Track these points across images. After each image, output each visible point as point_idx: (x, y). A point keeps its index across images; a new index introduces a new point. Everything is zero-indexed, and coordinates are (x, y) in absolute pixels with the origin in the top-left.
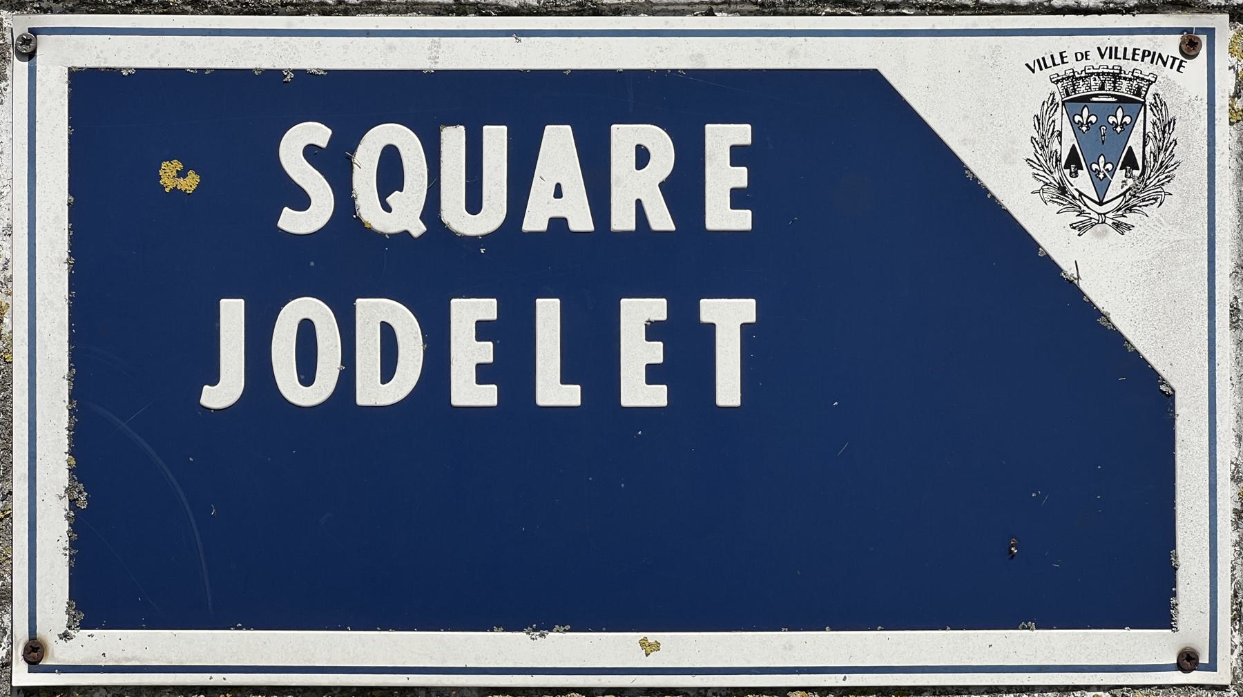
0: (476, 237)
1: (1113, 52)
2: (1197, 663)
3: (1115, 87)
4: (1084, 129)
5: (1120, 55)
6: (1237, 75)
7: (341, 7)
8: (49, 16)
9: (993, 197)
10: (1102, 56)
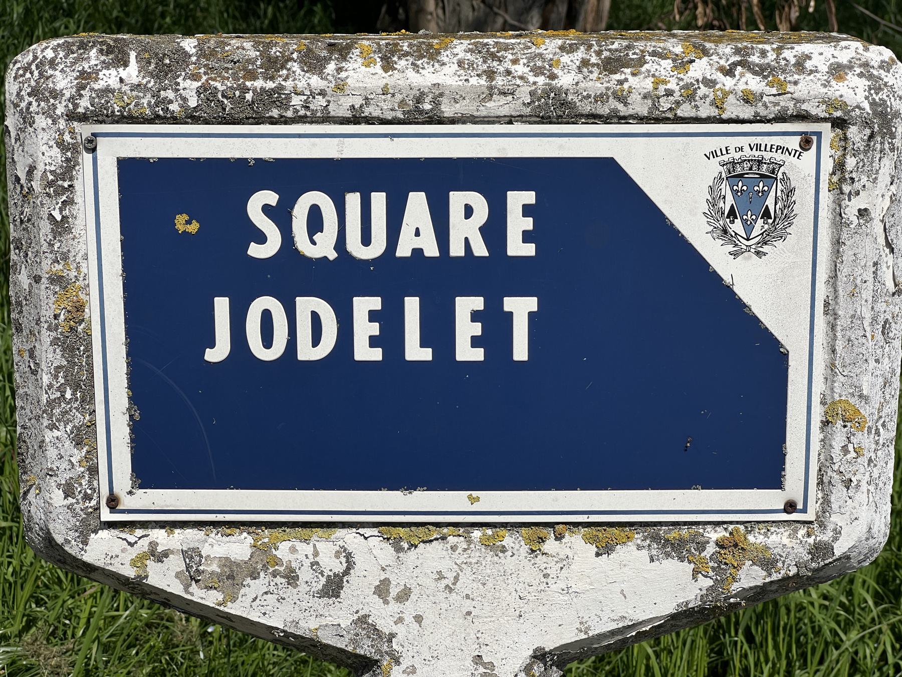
0: (367, 260)
1: (758, 147)
2: (796, 509)
3: (759, 169)
4: (739, 194)
5: (763, 148)
6: (834, 161)
7: (282, 119)
8: (103, 126)
9: (683, 235)
10: (752, 149)
